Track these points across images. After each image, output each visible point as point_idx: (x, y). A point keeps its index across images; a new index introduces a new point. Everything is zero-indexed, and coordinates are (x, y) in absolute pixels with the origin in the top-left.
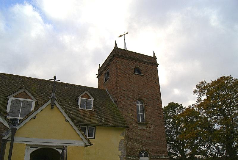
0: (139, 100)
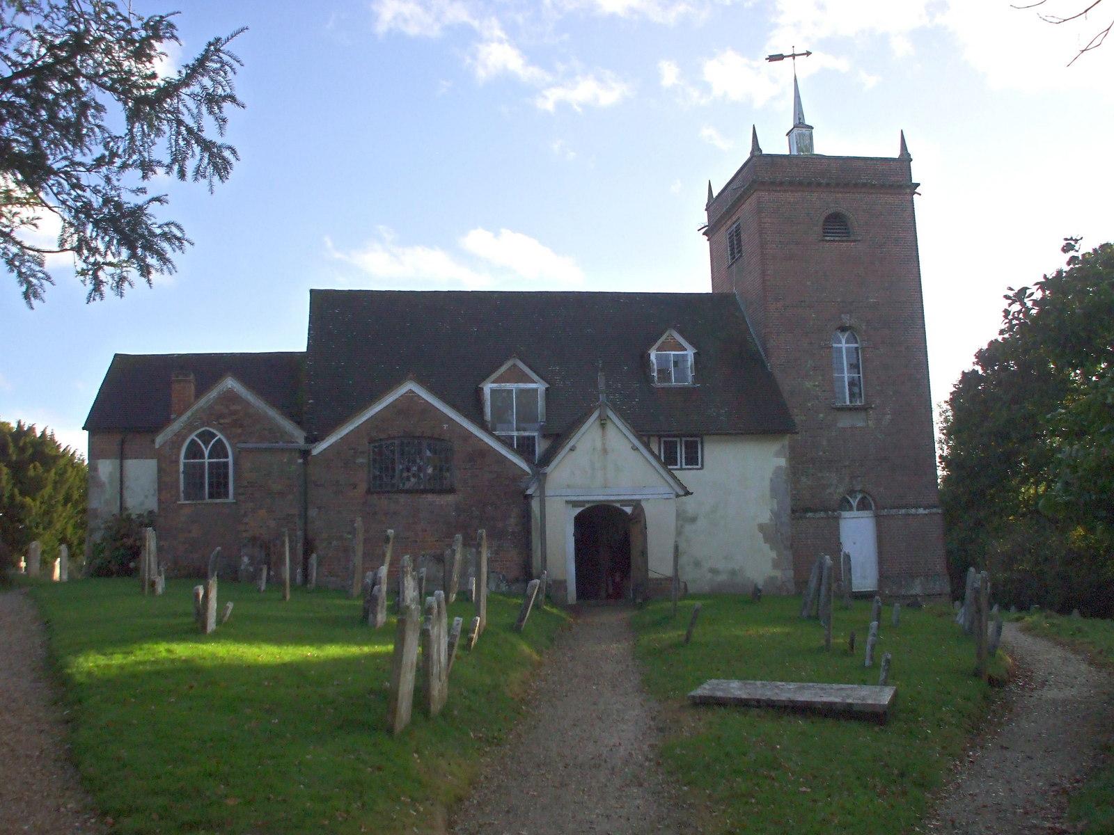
0: (843, 329)
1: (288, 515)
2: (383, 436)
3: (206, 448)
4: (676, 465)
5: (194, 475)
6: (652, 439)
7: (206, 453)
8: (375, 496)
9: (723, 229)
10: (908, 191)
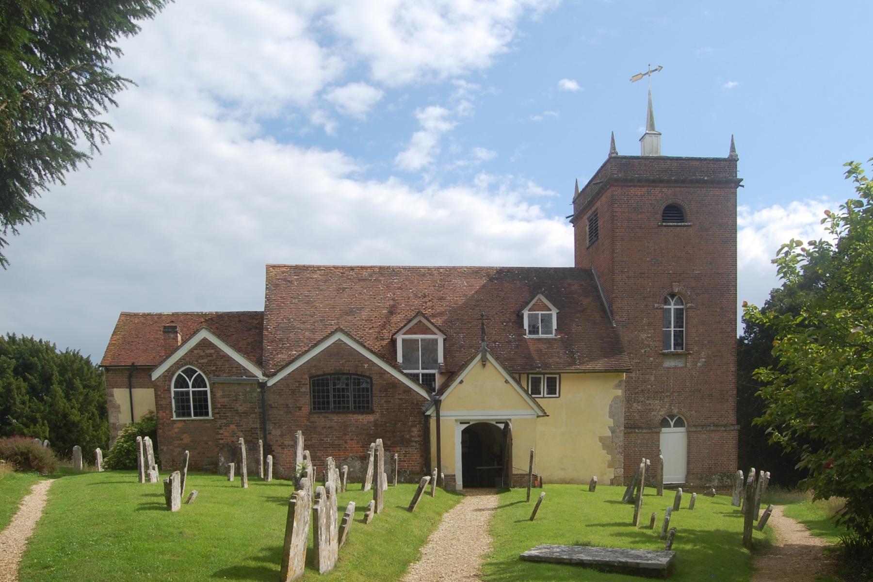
1: (252, 428)
2: (320, 373)
3: (190, 380)
5: (182, 399)
6: (522, 375)
7: (190, 384)
8: (315, 416)
9: (586, 217)
10: (733, 185)
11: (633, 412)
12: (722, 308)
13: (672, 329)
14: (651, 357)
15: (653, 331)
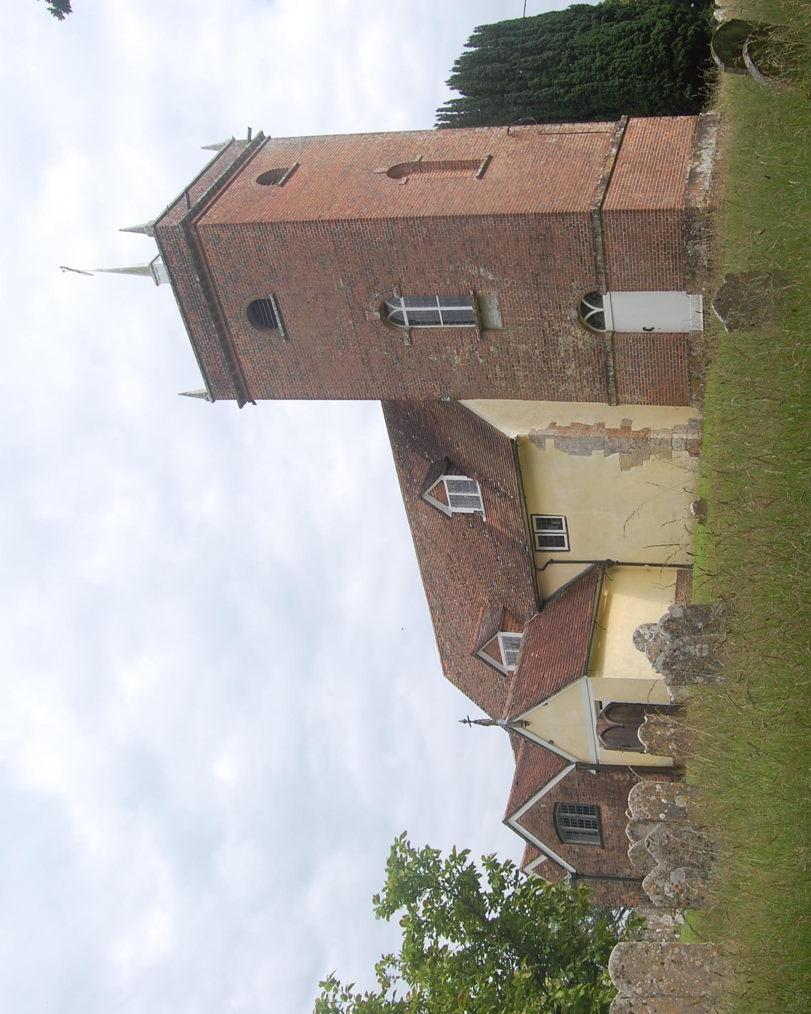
4: (564, 546)
6: (537, 567)
11: (580, 376)
12: (391, 243)
13: (439, 309)
14: (489, 350)
15: (447, 347)
